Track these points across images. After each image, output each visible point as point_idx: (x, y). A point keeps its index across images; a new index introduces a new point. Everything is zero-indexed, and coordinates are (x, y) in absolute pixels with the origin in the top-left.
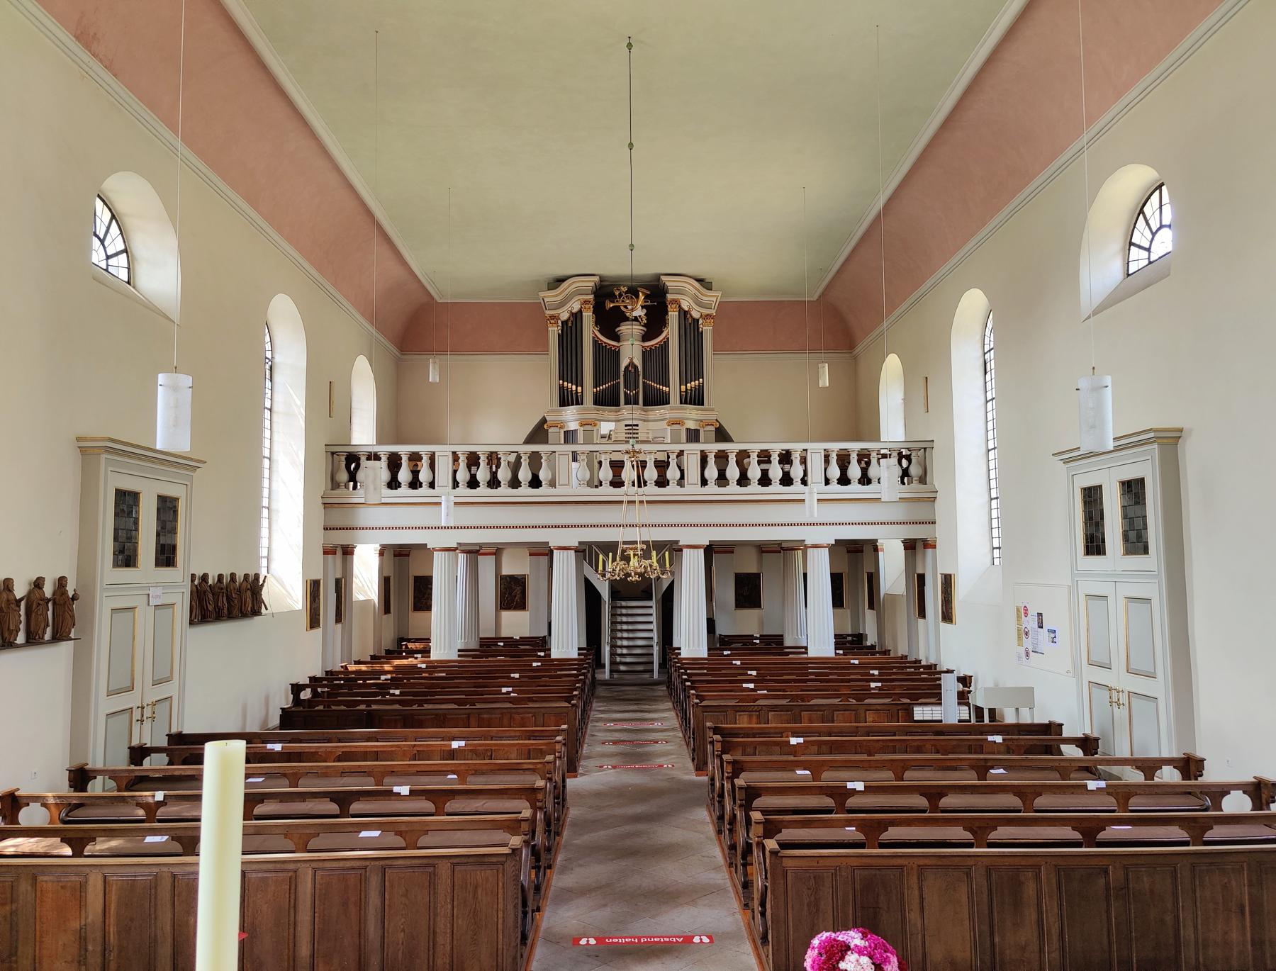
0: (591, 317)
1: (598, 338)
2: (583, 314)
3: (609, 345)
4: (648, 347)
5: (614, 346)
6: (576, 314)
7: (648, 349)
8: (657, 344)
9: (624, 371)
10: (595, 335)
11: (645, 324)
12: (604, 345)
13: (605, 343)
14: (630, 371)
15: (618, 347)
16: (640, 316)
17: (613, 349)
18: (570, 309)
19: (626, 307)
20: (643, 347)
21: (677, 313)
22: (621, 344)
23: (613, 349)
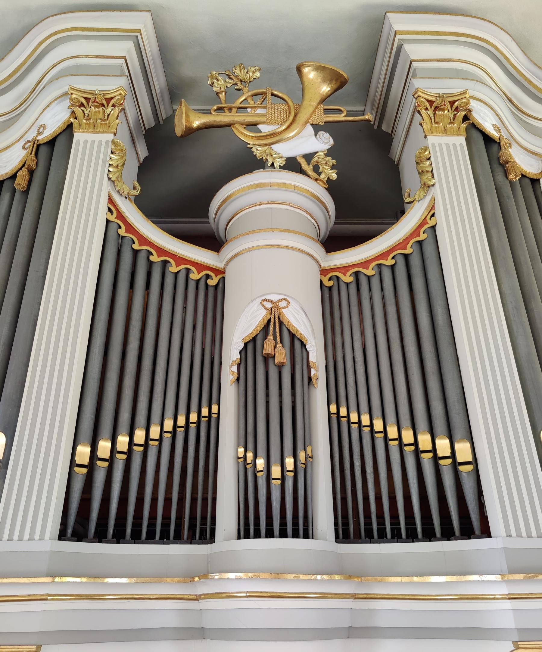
0: (105, 151)
1: (130, 228)
2: (78, 136)
3: (180, 260)
4: (344, 269)
5: (200, 267)
6: (52, 143)
7: (348, 278)
8: (384, 255)
9: (242, 363)
10: (121, 216)
11: (329, 181)
12: (154, 258)
13: (161, 251)
14: (267, 358)
15: (217, 271)
16: (309, 157)
17: (195, 276)
18: (31, 136)
19: (252, 126)
20: (324, 272)
21: (461, 140)
22: (228, 251)
23: (195, 276)
